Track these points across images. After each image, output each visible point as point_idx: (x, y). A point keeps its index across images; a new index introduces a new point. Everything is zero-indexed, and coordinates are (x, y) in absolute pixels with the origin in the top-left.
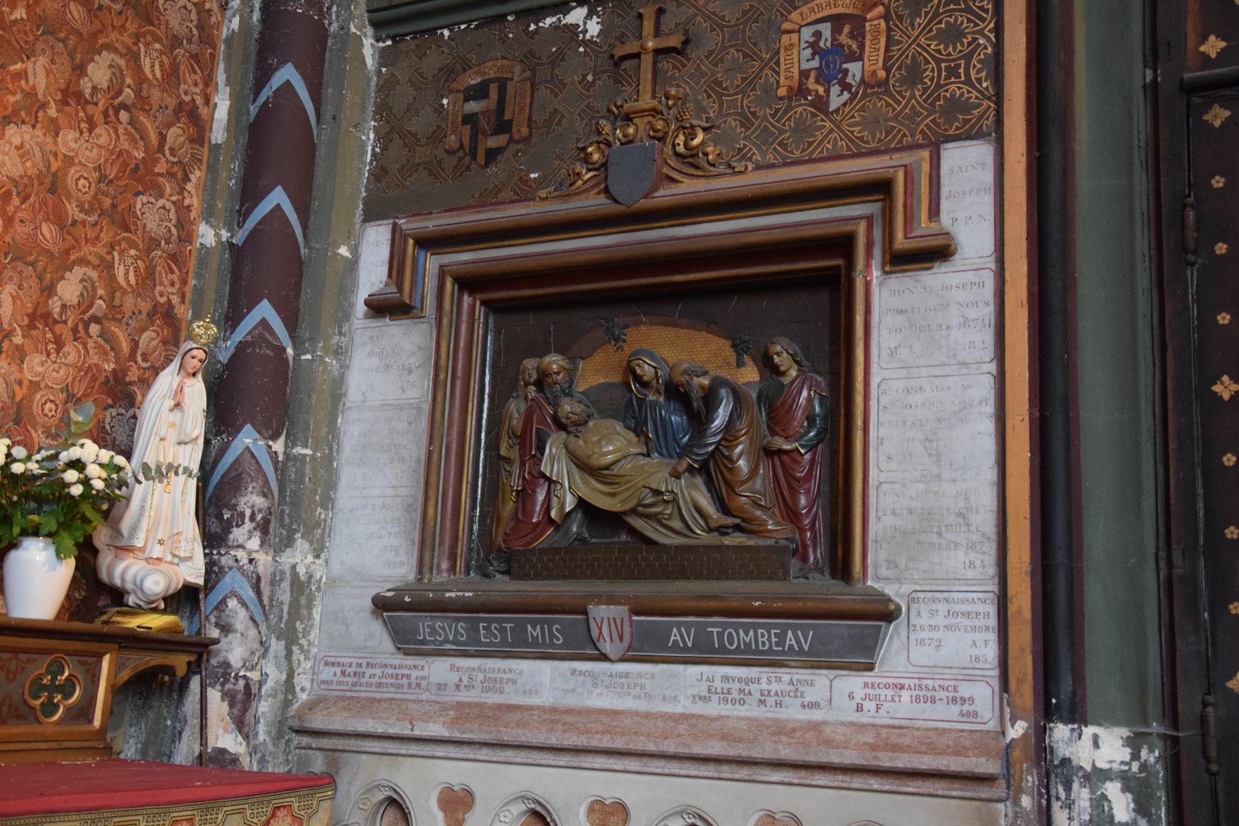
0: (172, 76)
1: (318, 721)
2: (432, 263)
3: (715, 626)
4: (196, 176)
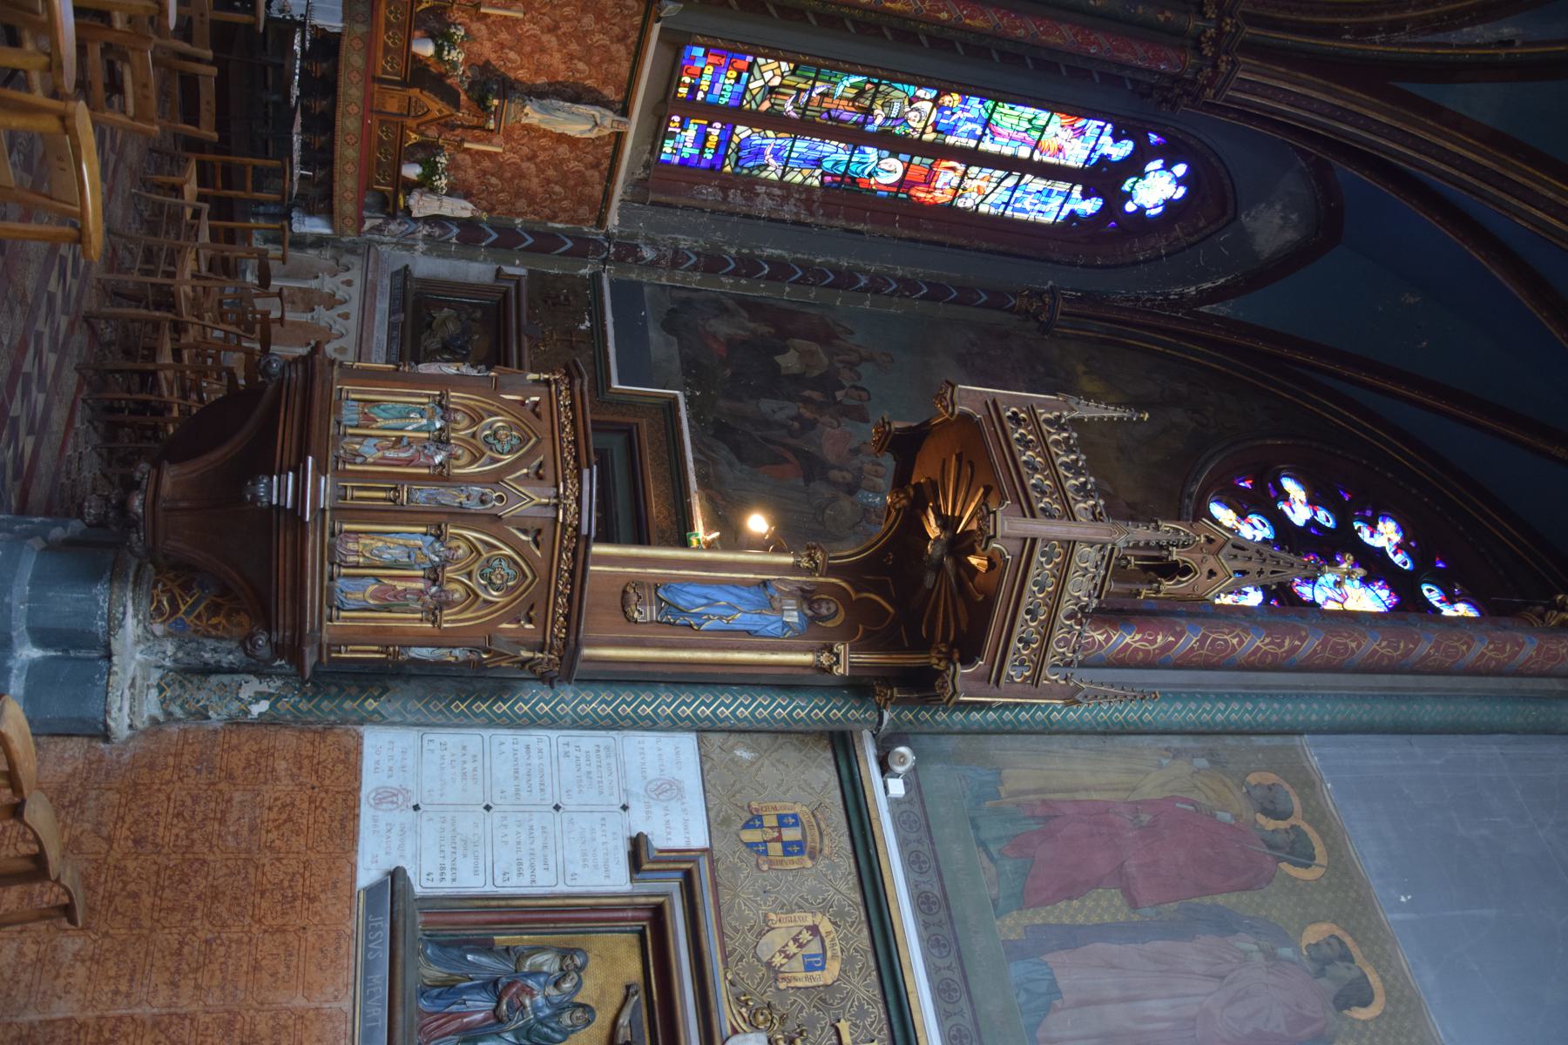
0: (564, 210)
1: (372, 250)
2: (512, 286)
3: (398, 341)
4: (537, 218)
